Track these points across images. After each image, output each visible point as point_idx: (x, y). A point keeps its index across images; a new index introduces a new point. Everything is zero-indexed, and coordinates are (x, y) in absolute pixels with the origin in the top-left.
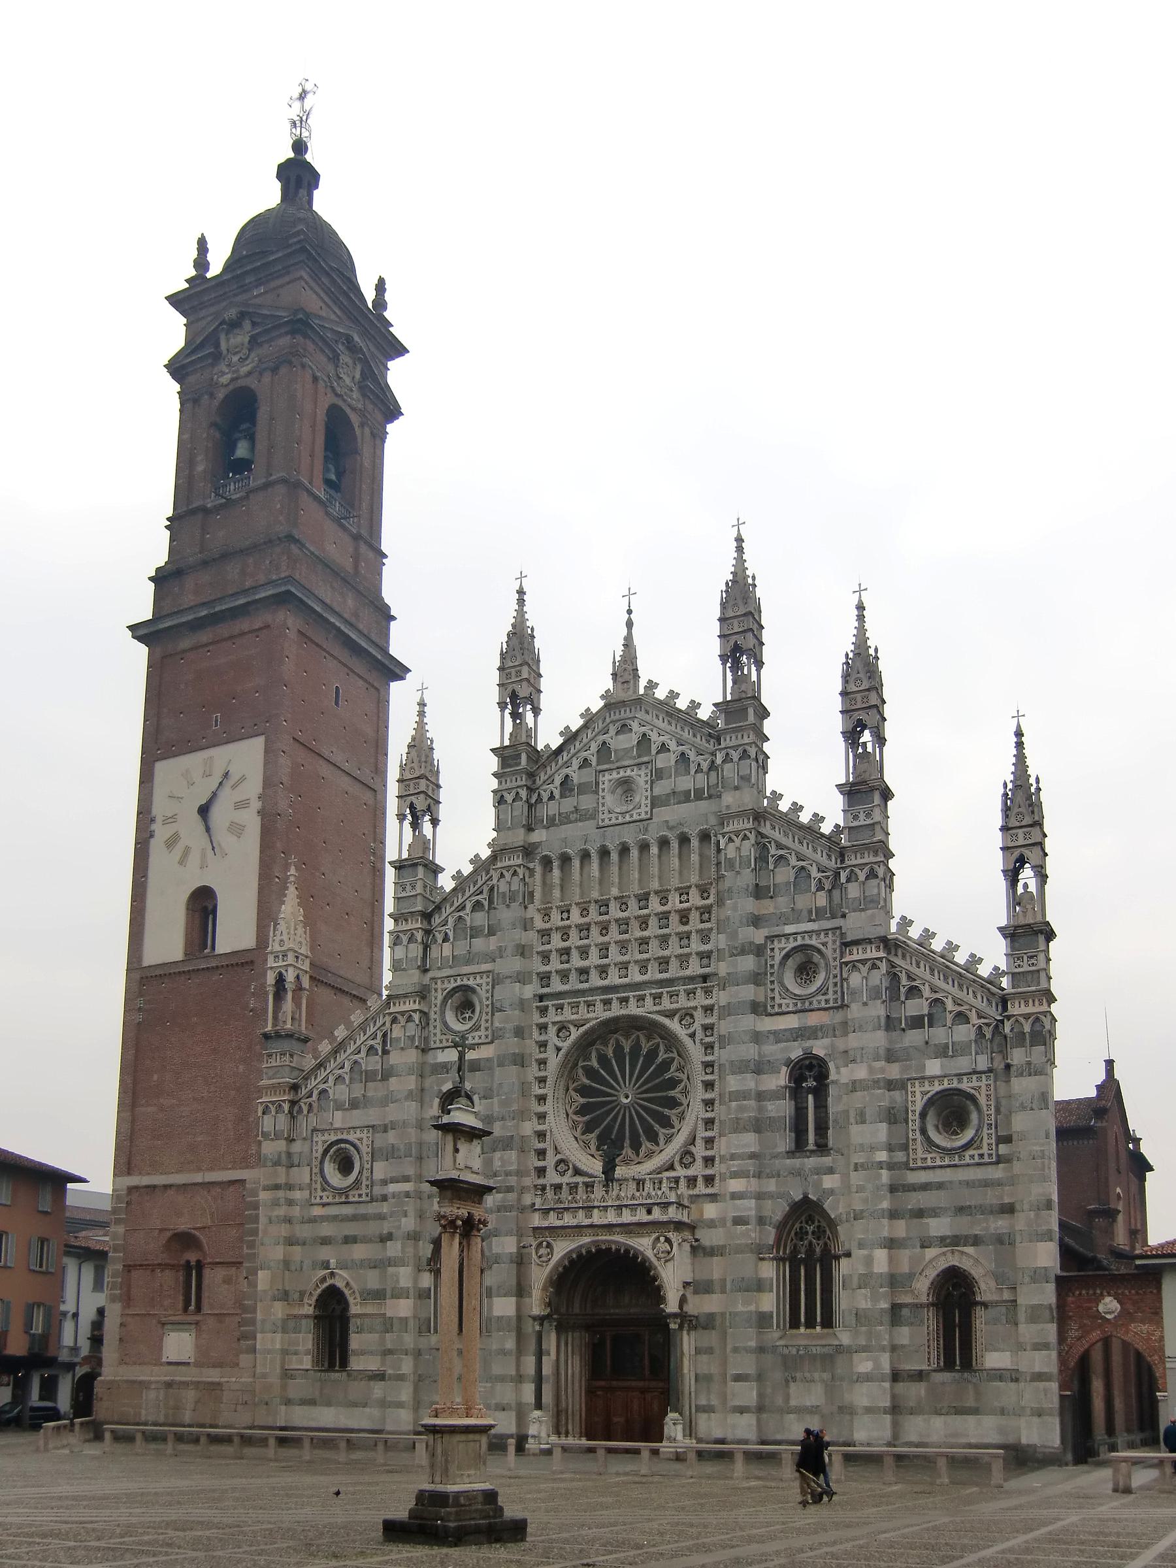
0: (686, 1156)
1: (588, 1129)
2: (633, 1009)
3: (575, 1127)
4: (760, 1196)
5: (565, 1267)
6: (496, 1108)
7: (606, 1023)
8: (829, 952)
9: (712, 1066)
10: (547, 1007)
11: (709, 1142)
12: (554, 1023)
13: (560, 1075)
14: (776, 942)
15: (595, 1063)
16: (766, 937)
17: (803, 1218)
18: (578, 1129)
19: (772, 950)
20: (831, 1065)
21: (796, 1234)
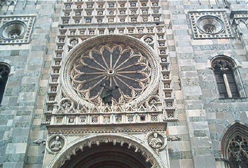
0: (154, 99)
1: (84, 87)
2: (116, 32)
3: (76, 85)
4: (210, 122)
5: (72, 156)
6: (26, 69)
7: (99, 38)
8: (222, 18)
9: (166, 58)
10: (66, 30)
11: (168, 93)
12: (69, 37)
13: (70, 59)
14: (194, 14)
15: (91, 56)
16: (190, 12)
17: (234, 137)
18: (78, 88)
19: (192, 17)
20: (236, 60)
21: (230, 147)
